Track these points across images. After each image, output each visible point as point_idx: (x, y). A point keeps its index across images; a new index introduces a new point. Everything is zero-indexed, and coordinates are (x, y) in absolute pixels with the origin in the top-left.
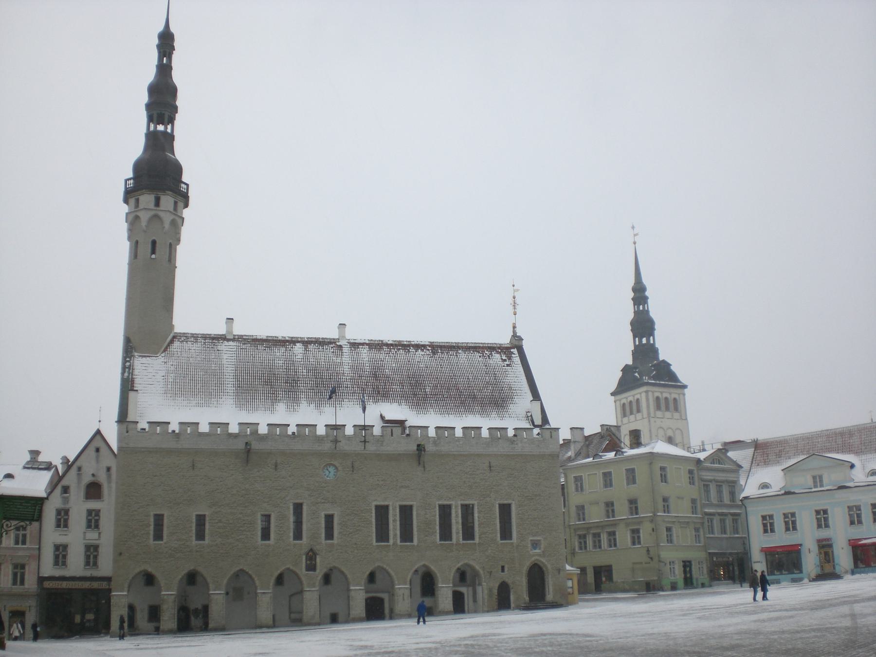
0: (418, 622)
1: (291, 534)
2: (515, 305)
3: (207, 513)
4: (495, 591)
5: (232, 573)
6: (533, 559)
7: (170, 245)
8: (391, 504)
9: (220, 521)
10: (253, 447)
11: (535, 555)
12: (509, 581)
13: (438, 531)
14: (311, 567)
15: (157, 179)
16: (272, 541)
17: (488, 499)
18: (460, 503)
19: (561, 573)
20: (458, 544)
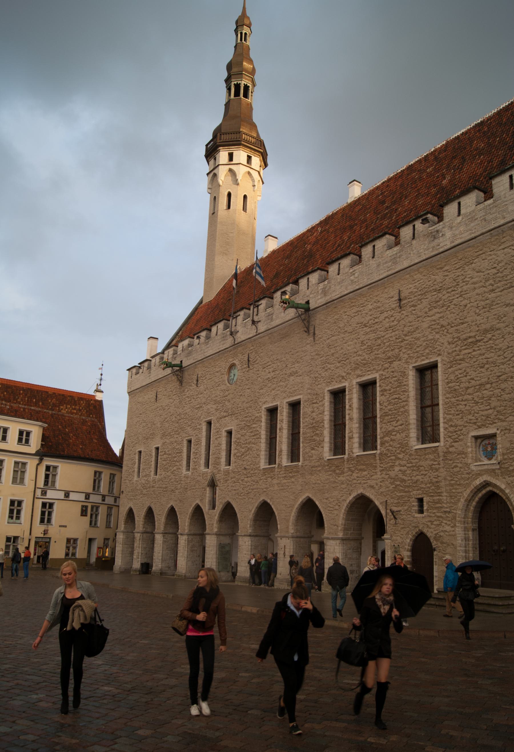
1: (202, 461)
3: (159, 445)
5: (167, 510)
6: (478, 482)
7: (229, 195)
8: (278, 403)
9: (165, 454)
12: (429, 535)
13: (327, 439)
16: (189, 473)
17: (396, 364)
18: (354, 382)
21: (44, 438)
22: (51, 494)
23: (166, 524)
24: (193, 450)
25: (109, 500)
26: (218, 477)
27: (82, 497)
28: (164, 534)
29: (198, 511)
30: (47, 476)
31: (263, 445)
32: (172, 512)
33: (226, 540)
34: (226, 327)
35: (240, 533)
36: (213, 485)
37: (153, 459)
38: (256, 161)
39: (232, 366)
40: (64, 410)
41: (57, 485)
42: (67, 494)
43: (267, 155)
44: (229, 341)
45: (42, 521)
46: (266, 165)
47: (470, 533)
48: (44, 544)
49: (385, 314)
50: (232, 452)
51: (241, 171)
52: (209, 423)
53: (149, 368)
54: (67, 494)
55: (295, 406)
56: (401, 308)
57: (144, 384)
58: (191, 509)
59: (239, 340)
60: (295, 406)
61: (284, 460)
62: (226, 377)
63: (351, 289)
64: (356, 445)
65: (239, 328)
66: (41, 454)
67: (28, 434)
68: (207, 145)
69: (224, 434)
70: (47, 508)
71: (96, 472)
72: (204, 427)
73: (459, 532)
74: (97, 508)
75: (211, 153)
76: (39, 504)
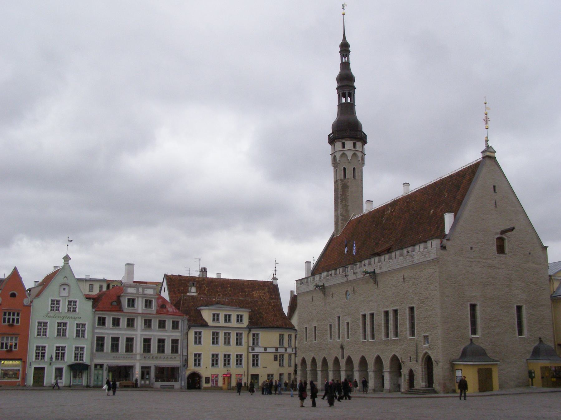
0: (263, 394)
1: (337, 336)
2: (486, 120)
4: (407, 377)
6: (424, 352)
7: (344, 169)
10: (326, 285)
11: (424, 347)
14: (343, 357)
15: (347, 131)
19: (440, 364)
20: (391, 340)
21: (250, 318)
22: (257, 350)
23: (322, 366)
24: (332, 330)
25: (289, 350)
26: (344, 344)
27: (273, 350)
28: (322, 371)
29: (336, 360)
30: (254, 339)
31: (361, 330)
32: (325, 361)
33: (349, 373)
34: (344, 271)
35: (354, 370)
36: (342, 348)
37: (313, 332)
38: (359, 144)
39: (347, 291)
40: (256, 294)
41: (260, 344)
42: (265, 349)
43: (366, 136)
44: (345, 279)
45: (253, 365)
46: (366, 143)
47: (424, 369)
48: (255, 377)
49: (400, 283)
50: (350, 333)
51: (349, 154)
52: (339, 317)
53: (307, 282)
54: (265, 349)
55: (372, 315)
56: (404, 281)
57: (305, 291)
58: (333, 359)
59: (349, 279)
60: (372, 315)
61: (369, 338)
62: (345, 296)
63: (389, 269)
64: (392, 335)
65: (349, 273)
66: (250, 328)
67: (242, 316)
68: (329, 136)
69: (346, 324)
70: (256, 358)
71: (280, 335)
72: (337, 319)
73: (420, 369)
74: (283, 355)
75: (332, 141)
76: (251, 356)
